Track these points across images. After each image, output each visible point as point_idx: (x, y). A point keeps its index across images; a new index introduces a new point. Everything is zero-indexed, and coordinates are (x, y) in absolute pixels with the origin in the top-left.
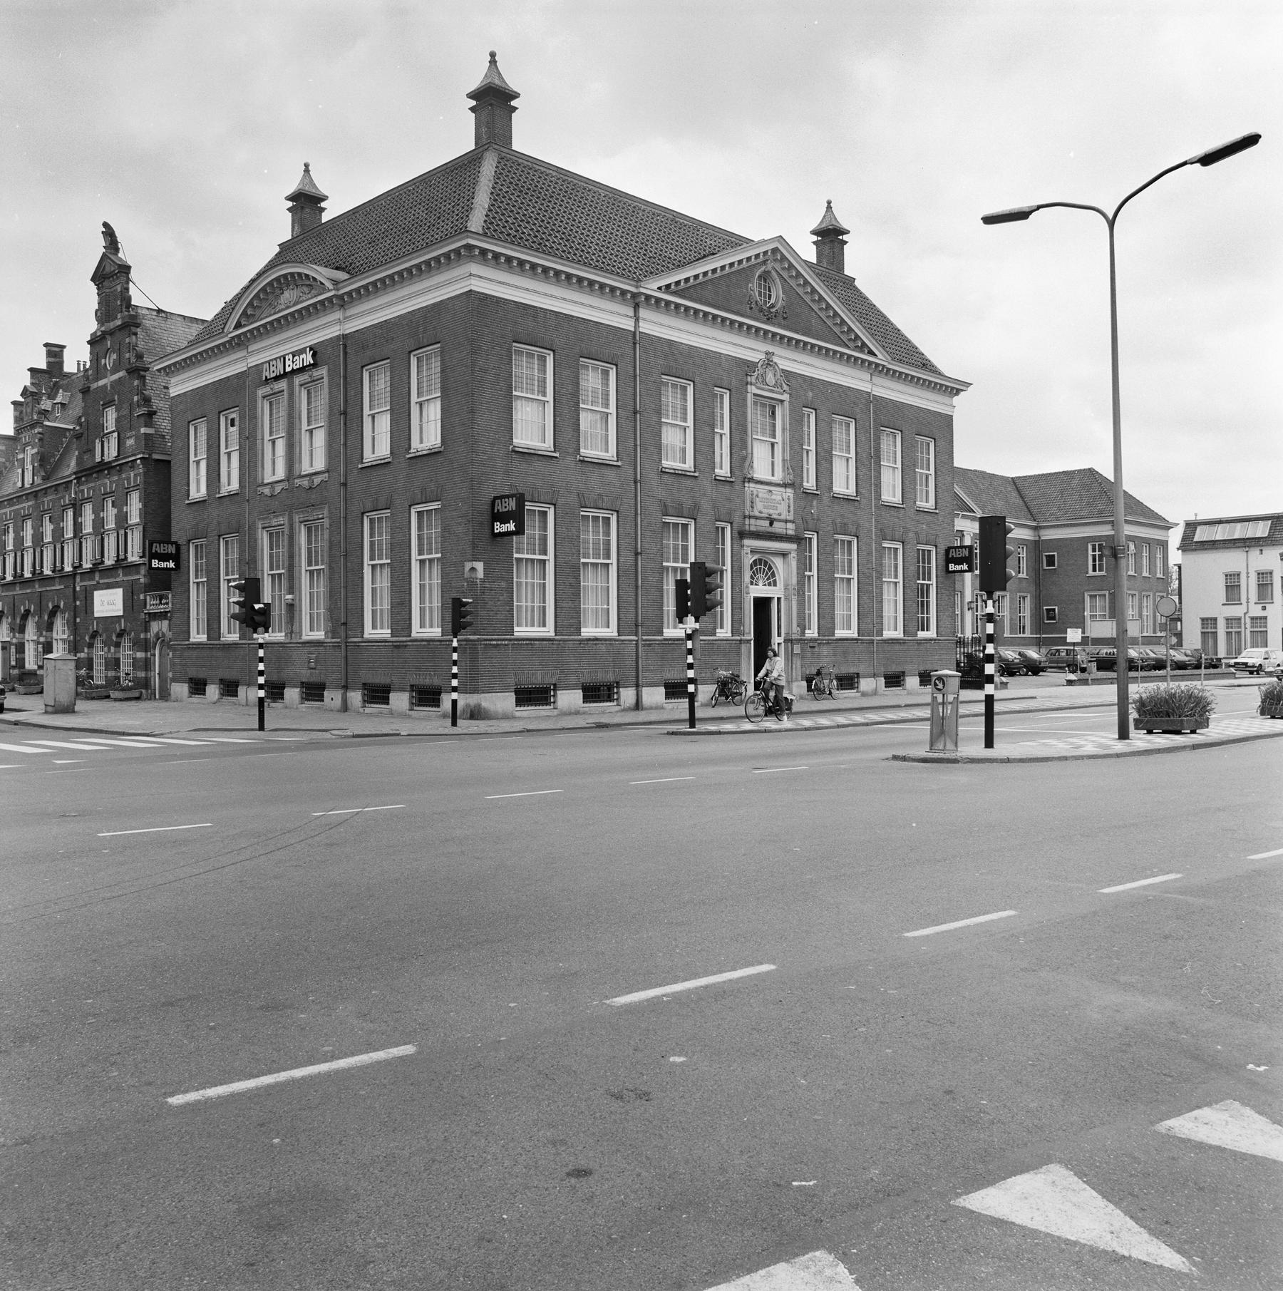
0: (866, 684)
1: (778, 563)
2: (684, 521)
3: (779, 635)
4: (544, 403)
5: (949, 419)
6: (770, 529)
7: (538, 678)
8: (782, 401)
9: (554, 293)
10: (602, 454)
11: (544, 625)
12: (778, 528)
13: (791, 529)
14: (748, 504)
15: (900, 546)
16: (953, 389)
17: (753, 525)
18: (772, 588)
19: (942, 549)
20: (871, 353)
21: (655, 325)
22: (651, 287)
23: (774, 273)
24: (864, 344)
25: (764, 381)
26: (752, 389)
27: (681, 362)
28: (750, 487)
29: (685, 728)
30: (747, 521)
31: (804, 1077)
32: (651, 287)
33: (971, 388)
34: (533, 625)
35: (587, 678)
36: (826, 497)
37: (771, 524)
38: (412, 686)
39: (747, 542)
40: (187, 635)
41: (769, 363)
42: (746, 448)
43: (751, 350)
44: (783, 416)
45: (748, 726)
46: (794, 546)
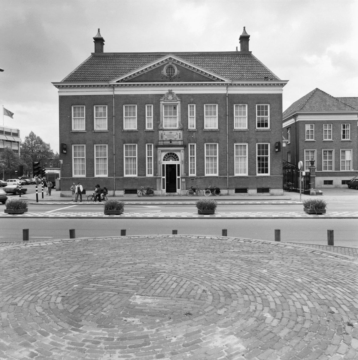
0: (250, 191)
1: (178, 154)
2: (215, 143)
3: (179, 175)
4: (194, 117)
5: (281, 94)
6: (171, 144)
7: (264, 186)
8: (178, 104)
9: (121, 90)
10: (244, 128)
11: (194, 173)
12: (174, 143)
13: (180, 143)
14: (160, 137)
15: (247, 144)
16: (282, 84)
17: (161, 143)
18: (177, 161)
19: (274, 143)
20: (118, 82)
21: (119, 92)
22: (114, 82)
23: (173, 65)
24: (218, 79)
25: (167, 99)
26: (162, 102)
27: (129, 100)
28: (160, 132)
29: (35, 202)
30: (159, 142)
31: (117, 315)
32: (114, 82)
33: (288, 82)
34: (80, 174)
35: (259, 186)
36: (200, 132)
37: (171, 142)
38: (96, 186)
39: (159, 148)
40: (94, 175)
41: (170, 93)
42: (160, 120)
43: (163, 91)
44: (179, 108)
45: (88, 203)
46: (183, 148)
